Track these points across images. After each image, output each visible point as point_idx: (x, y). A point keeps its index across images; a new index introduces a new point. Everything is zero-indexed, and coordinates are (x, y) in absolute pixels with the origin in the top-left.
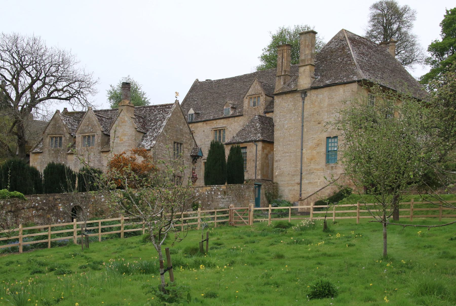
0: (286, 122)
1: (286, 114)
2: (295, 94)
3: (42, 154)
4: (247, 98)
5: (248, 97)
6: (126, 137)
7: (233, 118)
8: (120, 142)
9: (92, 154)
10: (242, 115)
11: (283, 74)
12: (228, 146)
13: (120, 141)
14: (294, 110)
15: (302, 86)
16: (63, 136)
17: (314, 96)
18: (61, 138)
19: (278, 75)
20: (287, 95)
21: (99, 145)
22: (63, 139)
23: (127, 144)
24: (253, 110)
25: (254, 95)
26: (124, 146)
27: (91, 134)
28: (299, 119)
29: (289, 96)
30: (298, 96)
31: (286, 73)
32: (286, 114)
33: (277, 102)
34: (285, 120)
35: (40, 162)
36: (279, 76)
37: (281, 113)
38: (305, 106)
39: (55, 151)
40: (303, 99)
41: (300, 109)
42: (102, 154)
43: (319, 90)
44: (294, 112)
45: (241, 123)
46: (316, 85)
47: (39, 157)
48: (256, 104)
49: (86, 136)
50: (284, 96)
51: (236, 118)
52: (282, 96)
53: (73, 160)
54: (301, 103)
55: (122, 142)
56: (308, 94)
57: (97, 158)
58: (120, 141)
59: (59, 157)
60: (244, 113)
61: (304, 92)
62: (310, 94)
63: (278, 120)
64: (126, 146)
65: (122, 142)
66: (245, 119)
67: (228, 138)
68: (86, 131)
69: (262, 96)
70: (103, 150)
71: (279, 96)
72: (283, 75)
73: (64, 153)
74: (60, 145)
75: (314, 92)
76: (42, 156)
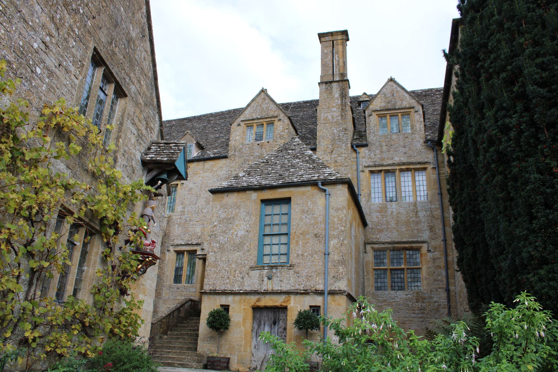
4: (239, 125)
5: (242, 124)
7: (201, 163)
10: (226, 157)
11: (337, 78)
12: (219, 195)
24: (256, 147)
25: (258, 119)
45: (223, 173)
48: (264, 136)
51: (209, 164)
60: (231, 153)
66: (232, 165)
67: (182, 204)
69: (280, 120)
72: (338, 81)
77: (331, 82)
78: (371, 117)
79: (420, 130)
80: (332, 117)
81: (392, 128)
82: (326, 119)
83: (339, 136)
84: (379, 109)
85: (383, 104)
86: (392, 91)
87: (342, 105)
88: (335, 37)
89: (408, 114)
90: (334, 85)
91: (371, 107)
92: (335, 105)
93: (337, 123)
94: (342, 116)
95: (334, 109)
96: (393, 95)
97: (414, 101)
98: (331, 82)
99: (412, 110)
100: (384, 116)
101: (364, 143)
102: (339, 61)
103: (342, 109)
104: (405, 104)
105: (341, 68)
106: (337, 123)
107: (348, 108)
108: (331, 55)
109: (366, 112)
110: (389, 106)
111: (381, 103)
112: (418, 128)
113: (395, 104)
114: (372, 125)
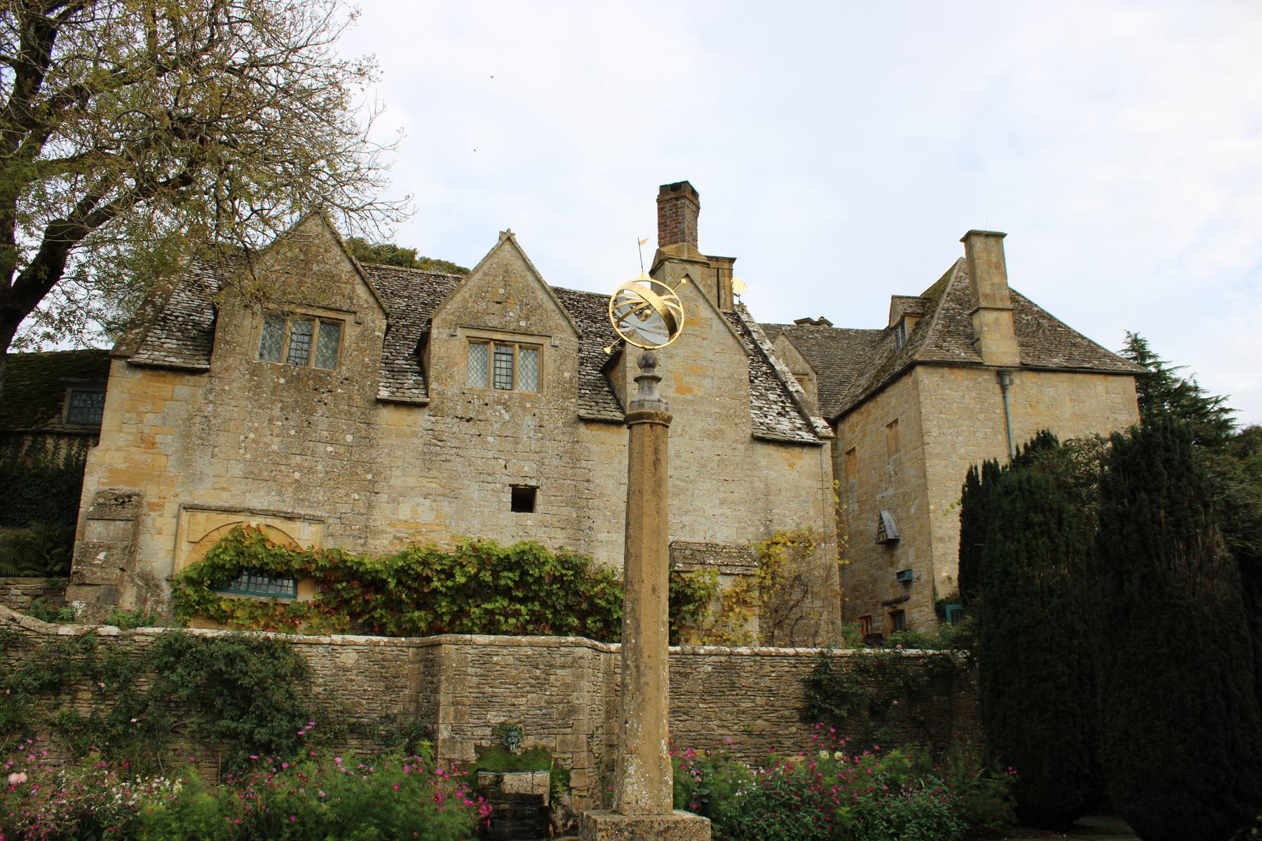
0: (960, 438)
1: (959, 418)
2: (977, 372)
3: (204, 379)
6: (707, 383)
8: (681, 397)
9: (530, 421)
13: (678, 390)
14: (980, 412)
15: (994, 358)
16: (349, 319)
17: (1032, 388)
18: (333, 326)
20: (956, 371)
21: (565, 390)
22: (351, 332)
23: (714, 410)
26: (694, 410)
27: (518, 338)
28: (1000, 437)
29: (961, 375)
30: (988, 381)
32: (959, 418)
33: (926, 382)
34: (958, 434)
35: (184, 415)
37: (941, 413)
38: (1010, 408)
39: (296, 381)
40: (1004, 389)
41: (998, 411)
42: (582, 429)
43: (1043, 375)
44: (981, 417)
46: (1029, 361)
47: (183, 388)
49: (486, 342)
50: (946, 372)
52: (940, 370)
53: (414, 434)
54: (999, 398)
55: (689, 397)
56: (1017, 381)
57: (556, 445)
58: (678, 390)
59: (320, 410)
61: (1001, 374)
62: (1022, 382)
63: (935, 432)
64: (708, 414)
65: (689, 397)
68: (494, 321)
70: (582, 412)
71: (930, 370)
73: (357, 398)
74: (335, 355)
75: (1029, 379)
76: (201, 391)
86: (784, 348)
88: (720, 265)
97: (808, 366)
108: (716, 288)
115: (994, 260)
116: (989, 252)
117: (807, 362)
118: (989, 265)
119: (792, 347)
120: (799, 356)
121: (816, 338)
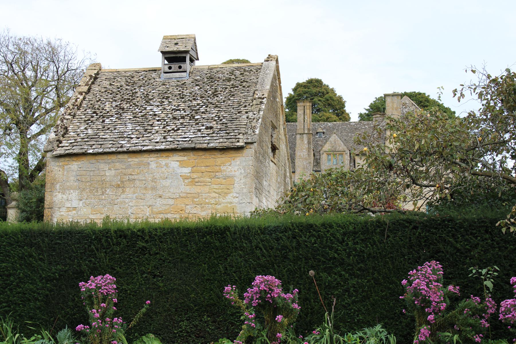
11: (306, 132)
19: (300, 132)
31: (311, 132)
36: (300, 134)
72: (307, 134)
77: (303, 134)
78: (323, 155)
79: (347, 165)
80: (303, 155)
81: (333, 162)
82: (300, 156)
83: (307, 166)
84: (327, 151)
85: (330, 148)
86: (335, 140)
87: (308, 148)
89: (342, 154)
90: (304, 135)
91: (323, 149)
92: (304, 148)
93: (306, 159)
94: (308, 155)
95: (304, 150)
96: (335, 143)
98: (303, 134)
99: (344, 153)
100: (330, 154)
101: (319, 169)
102: (307, 121)
103: (308, 151)
104: (341, 148)
105: (309, 125)
106: (306, 159)
107: (312, 150)
109: (321, 152)
110: (333, 149)
111: (329, 147)
112: (346, 163)
113: (335, 148)
114: (323, 160)
115: (395, 106)
116: (393, 103)
117: (345, 145)
118: (393, 109)
119: (339, 139)
120: (342, 143)
121: (366, 128)
